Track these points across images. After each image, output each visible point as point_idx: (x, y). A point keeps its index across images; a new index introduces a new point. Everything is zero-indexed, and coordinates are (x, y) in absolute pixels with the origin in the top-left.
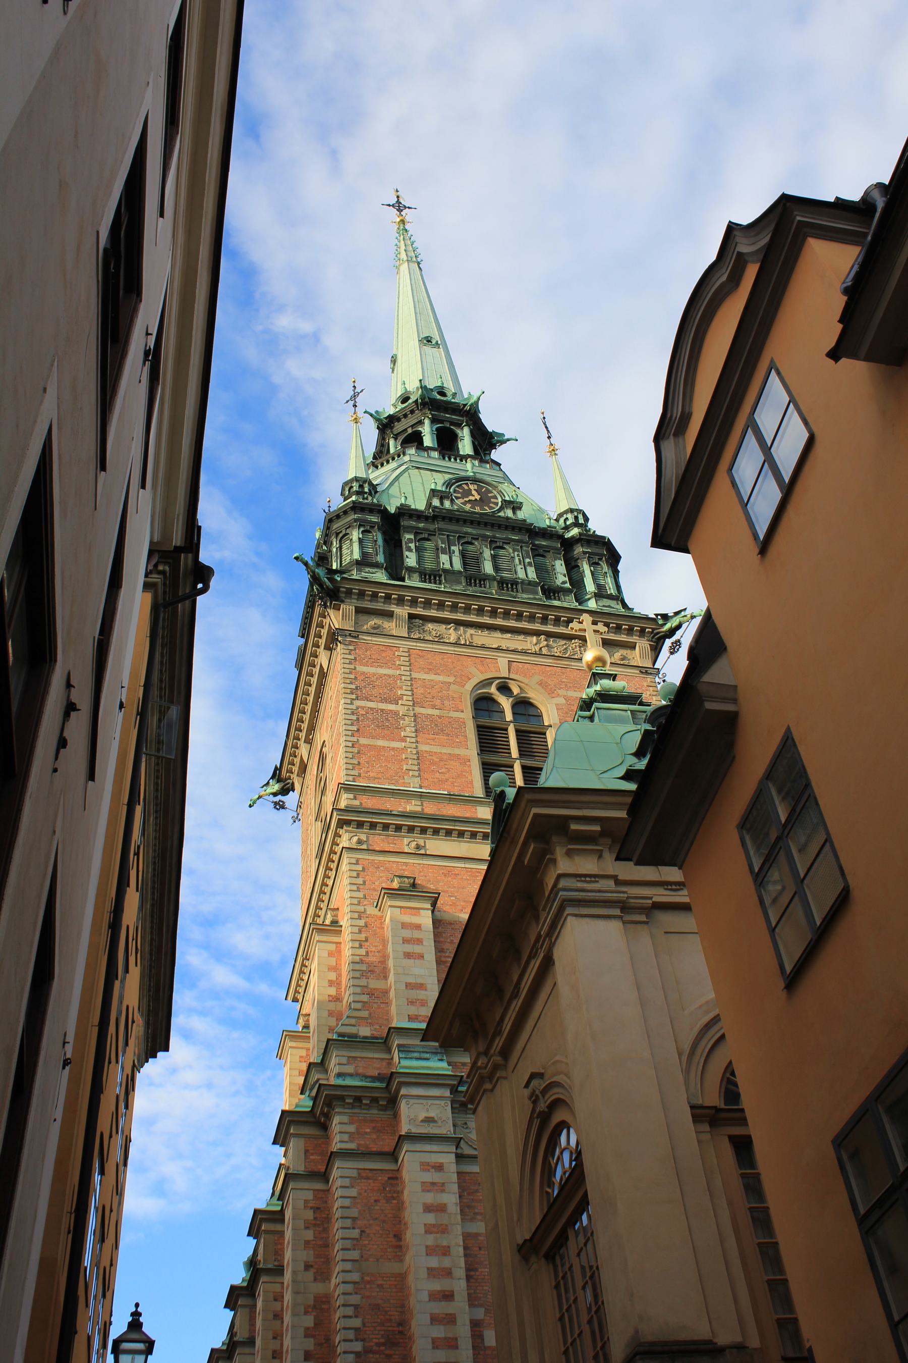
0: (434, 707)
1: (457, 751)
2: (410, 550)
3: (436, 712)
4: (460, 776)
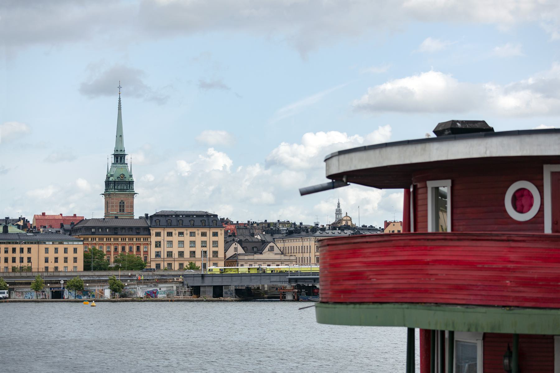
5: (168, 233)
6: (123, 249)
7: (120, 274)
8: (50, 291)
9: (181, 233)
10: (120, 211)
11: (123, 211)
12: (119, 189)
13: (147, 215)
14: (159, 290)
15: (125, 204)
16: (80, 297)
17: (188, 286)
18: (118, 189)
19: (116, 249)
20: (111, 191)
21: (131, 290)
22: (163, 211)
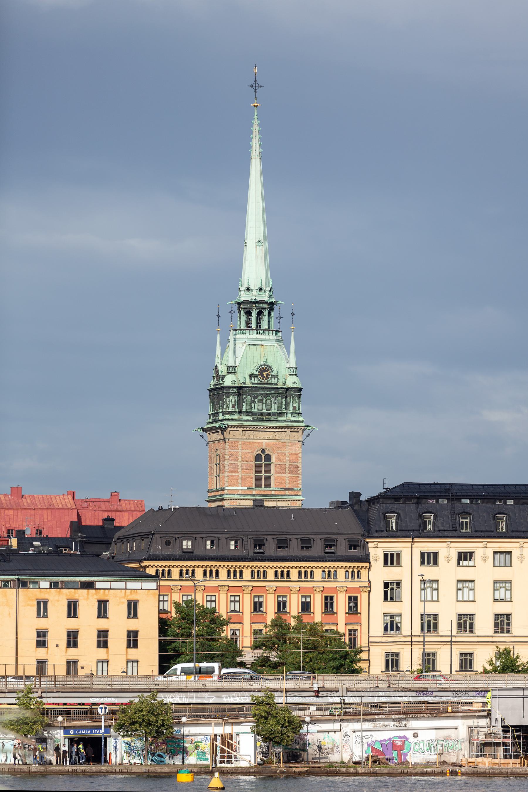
0: (246, 461)
1: (250, 475)
2: (244, 403)
3: (246, 463)
4: (250, 482)
5: (423, 554)
6: (282, 606)
7: (284, 686)
8: (65, 738)
9: (465, 553)
10: (258, 484)
11: (268, 484)
12: (254, 414)
13: (354, 496)
14: (412, 739)
15: (273, 460)
16: (162, 759)
17: (507, 727)
18: (248, 414)
19: (258, 606)
20: (229, 420)
21: (321, 736)
22: (409, 484)
